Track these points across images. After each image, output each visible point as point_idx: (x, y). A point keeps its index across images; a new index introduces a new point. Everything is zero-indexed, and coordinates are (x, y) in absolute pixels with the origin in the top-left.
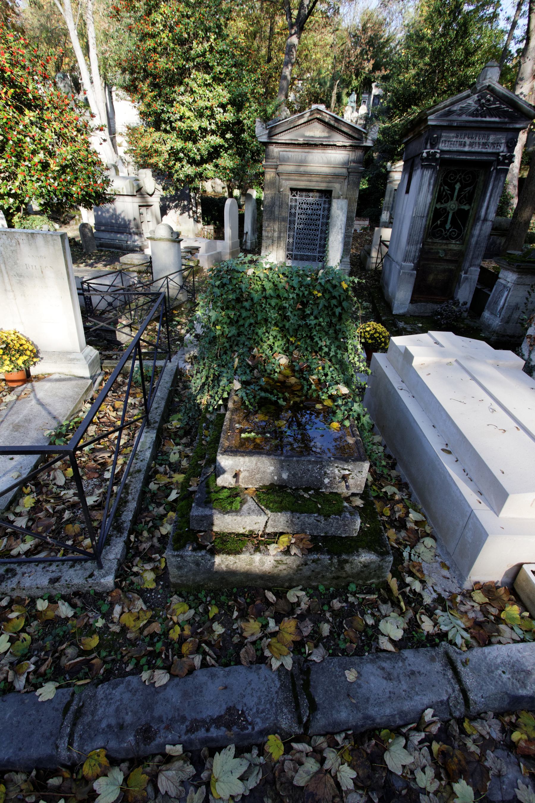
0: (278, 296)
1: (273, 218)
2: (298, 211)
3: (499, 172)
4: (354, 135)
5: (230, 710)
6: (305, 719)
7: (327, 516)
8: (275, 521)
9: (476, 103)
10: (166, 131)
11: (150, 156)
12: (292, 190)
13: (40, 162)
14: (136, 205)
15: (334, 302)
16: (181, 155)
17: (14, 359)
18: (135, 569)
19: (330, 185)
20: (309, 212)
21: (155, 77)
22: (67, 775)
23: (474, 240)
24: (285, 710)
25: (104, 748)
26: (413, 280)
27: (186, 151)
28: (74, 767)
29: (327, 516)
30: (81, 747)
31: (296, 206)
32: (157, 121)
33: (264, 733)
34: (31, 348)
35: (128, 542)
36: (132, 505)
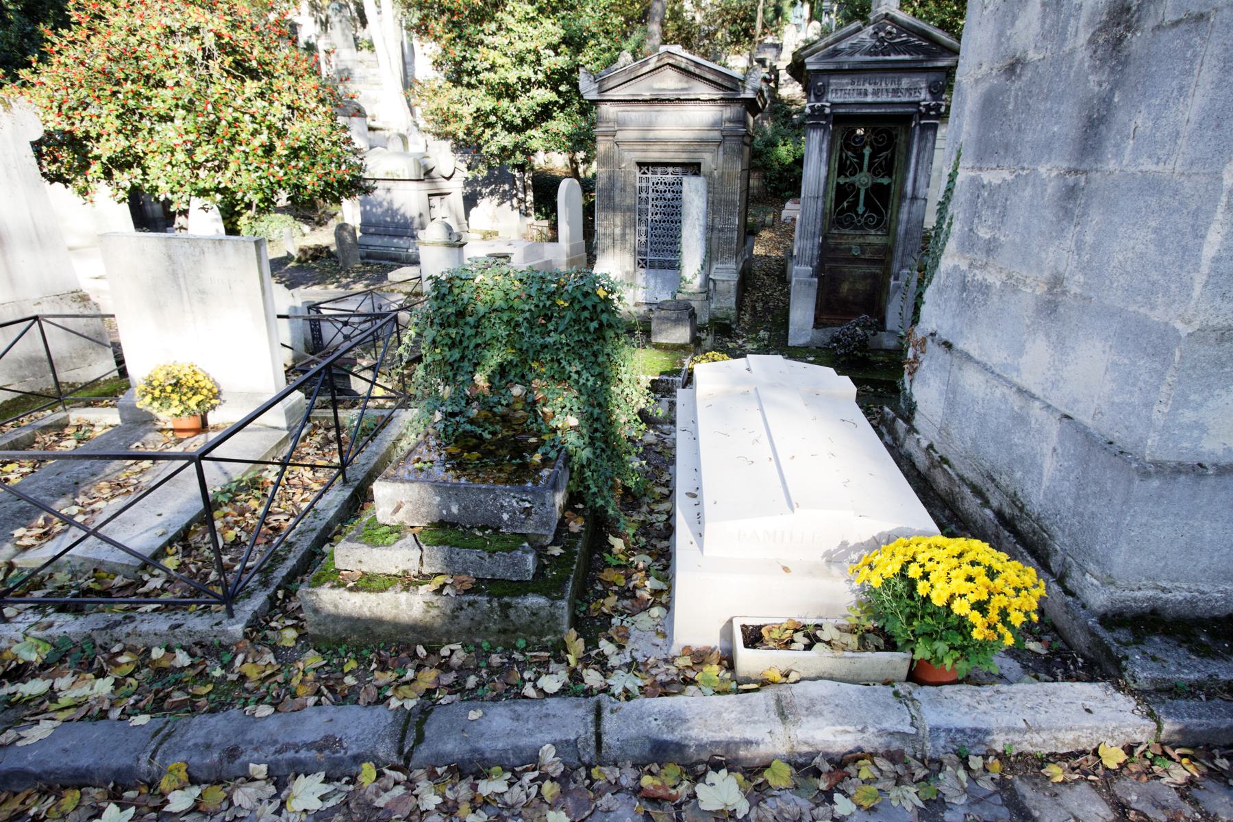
0: (511, 308)
1: (612, 207)
2: (651, 195)
3: (924, 128)
4: (725, 83)
5: (326, 738)
6: (406, 750)
7: (492, 553)
8: (430, 557)
9: (871, 37)
10: (469, 86)
11: (446, 121)
12: (640, 165)
13: (262, 146)
14: (425, 194)
15: (586, 314)
16: (493, 119)
17: (184, 398)
18: (273, 624)
19: (696, 155)
20: (669, 195)
21: (452, 12)
22: (144, 790)
23: (901, 229)
24: (387, 740)
25: (186, 762)
26: (813, 292)
27: (499, 114)
28: (152, 785)
29: (492, 553)
30: (162, 761)
31: (647, 188)
32: (459, 75)
33: (358, 759)
34: (209, 386)
35: (272, 598)
36: (291, 562)
